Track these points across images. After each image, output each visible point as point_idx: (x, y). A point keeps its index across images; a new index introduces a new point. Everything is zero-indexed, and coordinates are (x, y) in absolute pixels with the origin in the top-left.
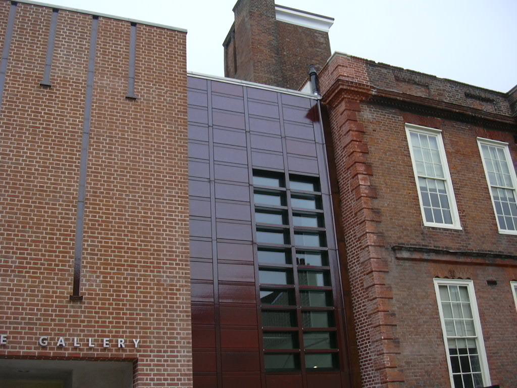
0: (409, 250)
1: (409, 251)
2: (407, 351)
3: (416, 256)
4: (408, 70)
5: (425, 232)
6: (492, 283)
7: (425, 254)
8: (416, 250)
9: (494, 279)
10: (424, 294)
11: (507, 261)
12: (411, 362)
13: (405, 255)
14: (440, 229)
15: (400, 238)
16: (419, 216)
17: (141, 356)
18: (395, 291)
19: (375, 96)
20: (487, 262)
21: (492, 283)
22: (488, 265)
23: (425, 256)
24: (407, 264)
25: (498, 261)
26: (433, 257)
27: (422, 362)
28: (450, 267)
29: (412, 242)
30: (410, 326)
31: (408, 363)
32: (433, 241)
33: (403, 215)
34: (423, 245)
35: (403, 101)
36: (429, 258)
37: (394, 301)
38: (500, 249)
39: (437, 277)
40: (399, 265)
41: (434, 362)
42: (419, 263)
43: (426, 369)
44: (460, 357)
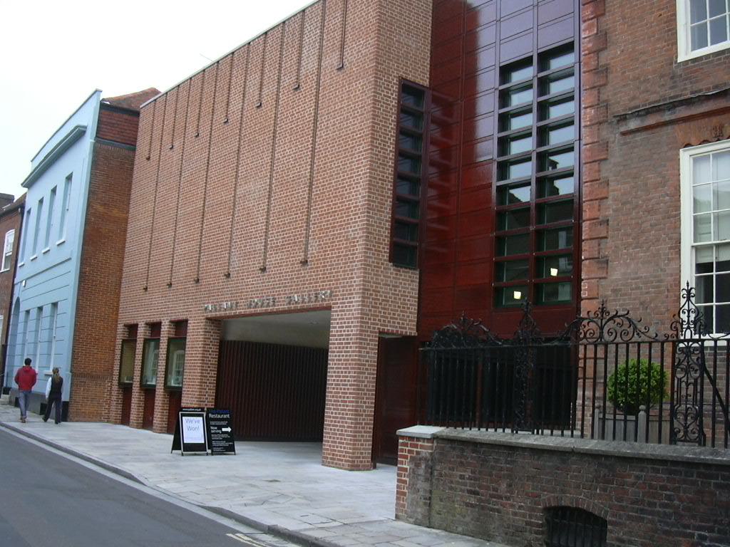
0: (638, 114)
1: (638, 116)
2: (617, 273)
3: (651, 120)
7: (668, 113)
8: (648, 112)
10: (659, 179)
12: (620, 290)
13: (633, 124)
14: (707, 56)
15: (634, 98)
16: (671, 50)
17: (334, 304)
18: (613, 185)
23: (667, 117)
24: (639, 137)
26: (682, 112)
27: (637, 288)
28: (715, 120)
29: (653, 97)
30: (629, 235)
31: (614, 291)
32: (691, 83)
33: (644, 58)
34: (671, 98)
36: (673, 117)
37: (610, 202)
39: (688, 145)
40: (626, 144)
41: (658, 287)
42: (658, 129)
43: (642, 300)
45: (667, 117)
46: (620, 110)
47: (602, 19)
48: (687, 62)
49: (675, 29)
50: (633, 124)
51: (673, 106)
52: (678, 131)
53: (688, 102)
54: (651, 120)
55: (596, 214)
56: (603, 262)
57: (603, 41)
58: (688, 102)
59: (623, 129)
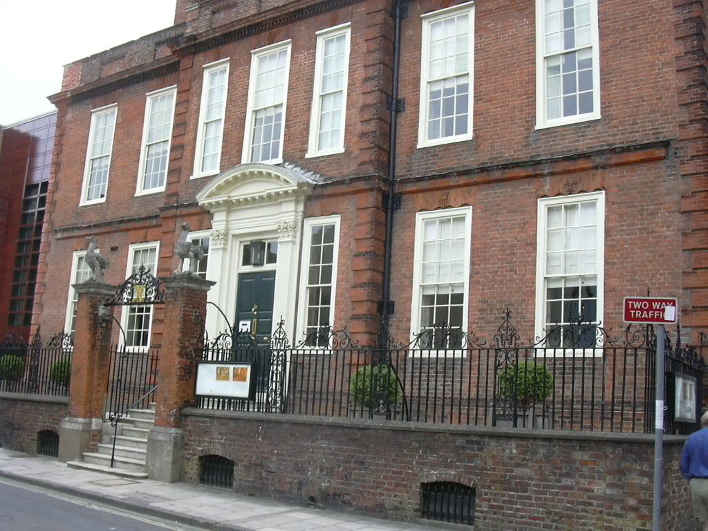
3: (66, 235)
4: (111, 49)
5: (79, 211)
6: (114, 249)
7: (71, 232)
9: (116, 245)
11: (130, 225)
13: (59, 236)
19: (72, 96)
20: (113, 229)
21: (114, 249)
22: (114, 232)
23: (71, 234)
25: (123, 226)
29: (69, 223)
34: (75, 224)
35: (88, 91)
37: (47, 274)
38: (131, 213)
39: (76, 250)
44: (447, 307)
45: (71, 234)
46: (57, 226)
47: (58, 174)
48: (85, 206)
49: (81, 188)
50: (59, 236)
51: (73, 229)
52: (74, 242)
53: (78, 228)
54: (66, 235)
55: (41, 280)
56: (41, 306)
57: (56, 184)
58: (78, 228)
59: (56, 237)
